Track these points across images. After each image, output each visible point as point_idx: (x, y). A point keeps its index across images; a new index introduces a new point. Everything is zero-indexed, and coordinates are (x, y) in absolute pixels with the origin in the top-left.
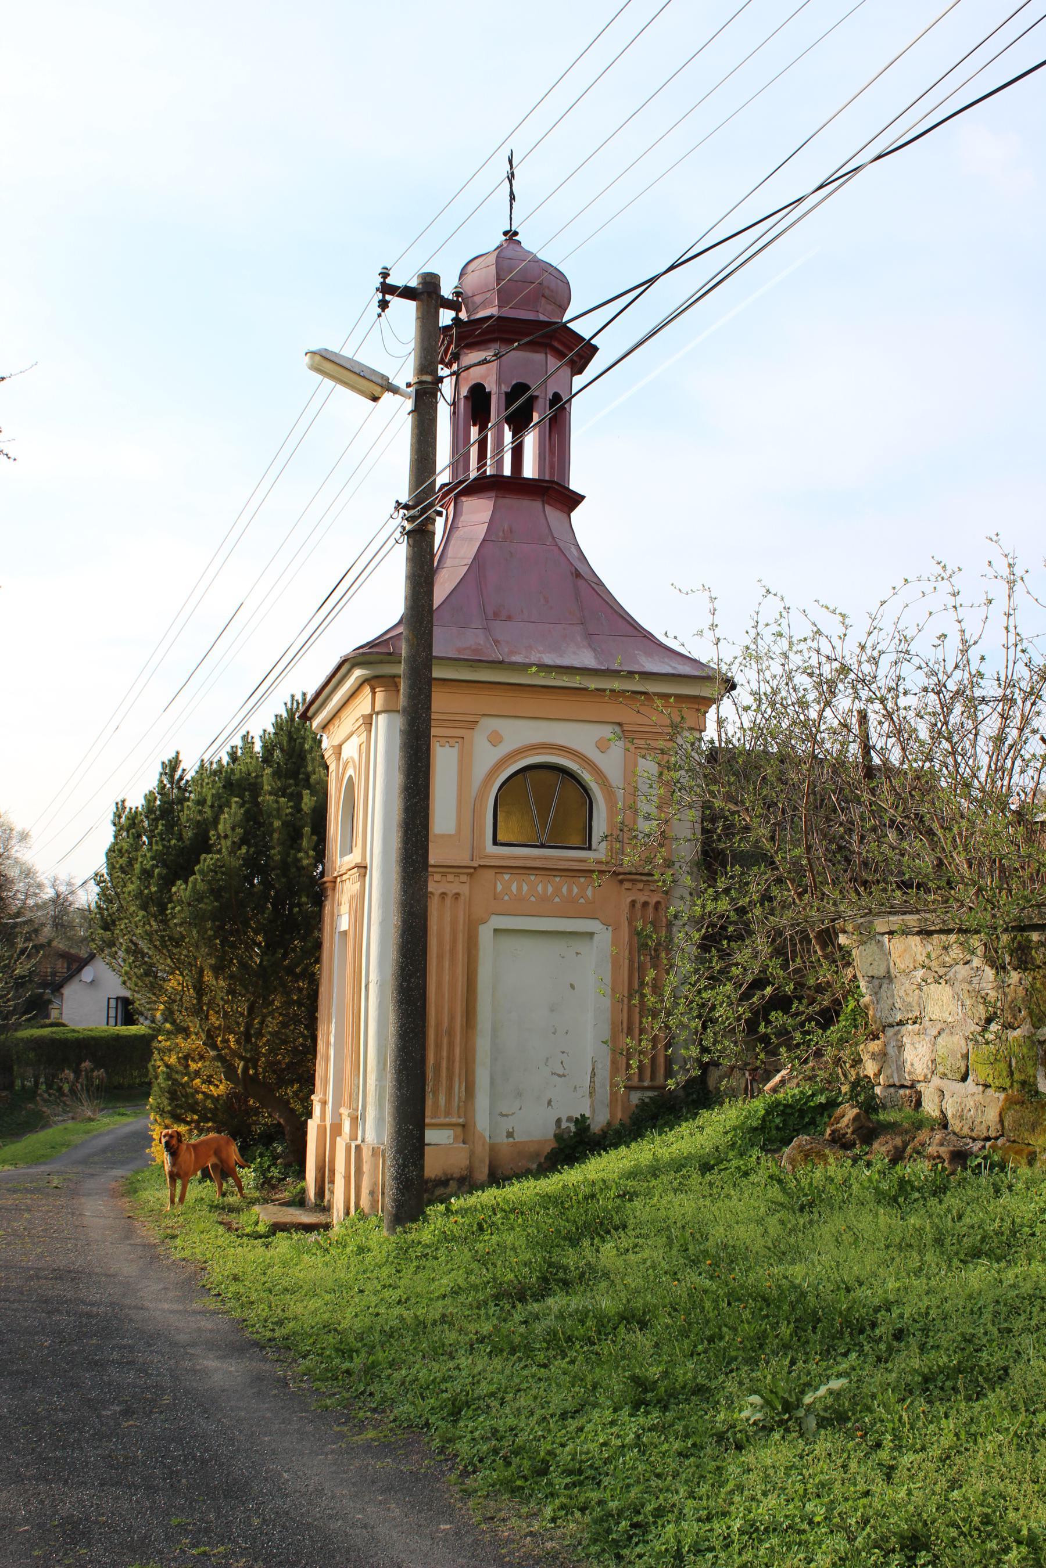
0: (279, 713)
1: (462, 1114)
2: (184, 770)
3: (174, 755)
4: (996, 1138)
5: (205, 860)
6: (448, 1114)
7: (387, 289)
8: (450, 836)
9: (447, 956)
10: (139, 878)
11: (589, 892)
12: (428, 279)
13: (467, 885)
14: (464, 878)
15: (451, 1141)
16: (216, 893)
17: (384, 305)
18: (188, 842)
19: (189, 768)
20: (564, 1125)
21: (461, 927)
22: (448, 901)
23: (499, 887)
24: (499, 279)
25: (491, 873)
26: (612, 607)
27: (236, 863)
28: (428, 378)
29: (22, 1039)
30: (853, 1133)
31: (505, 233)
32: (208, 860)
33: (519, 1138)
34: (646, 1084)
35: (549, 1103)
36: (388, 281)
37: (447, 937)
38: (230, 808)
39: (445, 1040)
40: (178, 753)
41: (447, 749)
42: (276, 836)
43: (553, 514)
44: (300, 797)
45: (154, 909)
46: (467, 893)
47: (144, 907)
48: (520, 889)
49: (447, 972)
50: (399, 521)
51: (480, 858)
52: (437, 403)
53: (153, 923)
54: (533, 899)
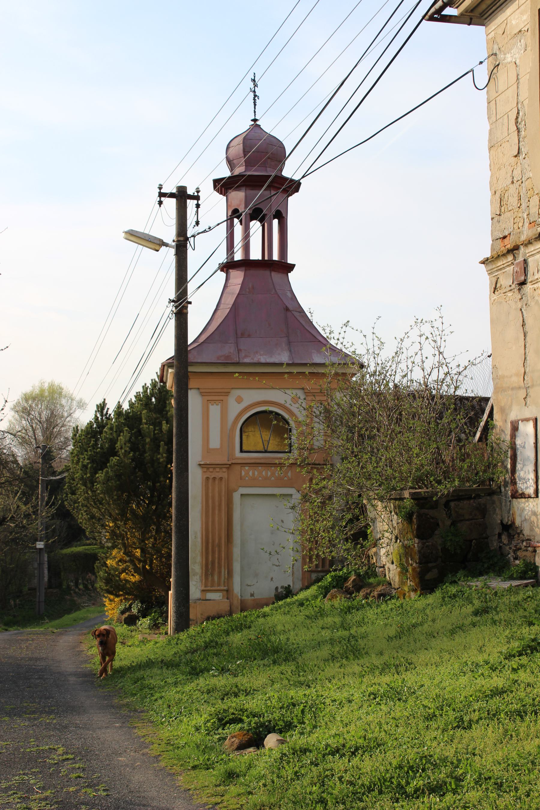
0: (153, 378)
1: (226, 585)
2: (108, 409)
3: (103, 400)
4: (398, 589)
5: (112, 460)
6: (219, 585)
7: (161, 195)
9: (217, 508)
10: (81, 470)
11: (289, 474)
12: (180, 190)
13: (226, 473)
14: (224, 470)
15: (221, 598)
16: (118, 476)
17: (160, 203)
18: (105, 450)
19: (111, 408)
20: (280, 590)
21: (223, 493)
22: (217, 482)
23: (243, 473)
24: (245, 152)
25: (238, 467)
27: (127, 461)
28: (182, 239)
29: (66, 554)
30: (352, 587)
31: (252, 120)
32: (114, 460)
33: (256, 596)
34: (319, 569)
35: (272, 579)
36: (162, 191)
37: (217, 498)
38: (123, 433)
39: (217, 549)
40: (105, 400)
42: (147, 446)
43: (276, 276)
44: (160, 424)
45: (89, 485)
46: (226, 477)
47: (85, 484)
48: (253, 474)
49: (217, 516)
50: (171, 307)
51: (233, 459)
52: (187, 250)
53: (90, 492)
54: (260, 479)
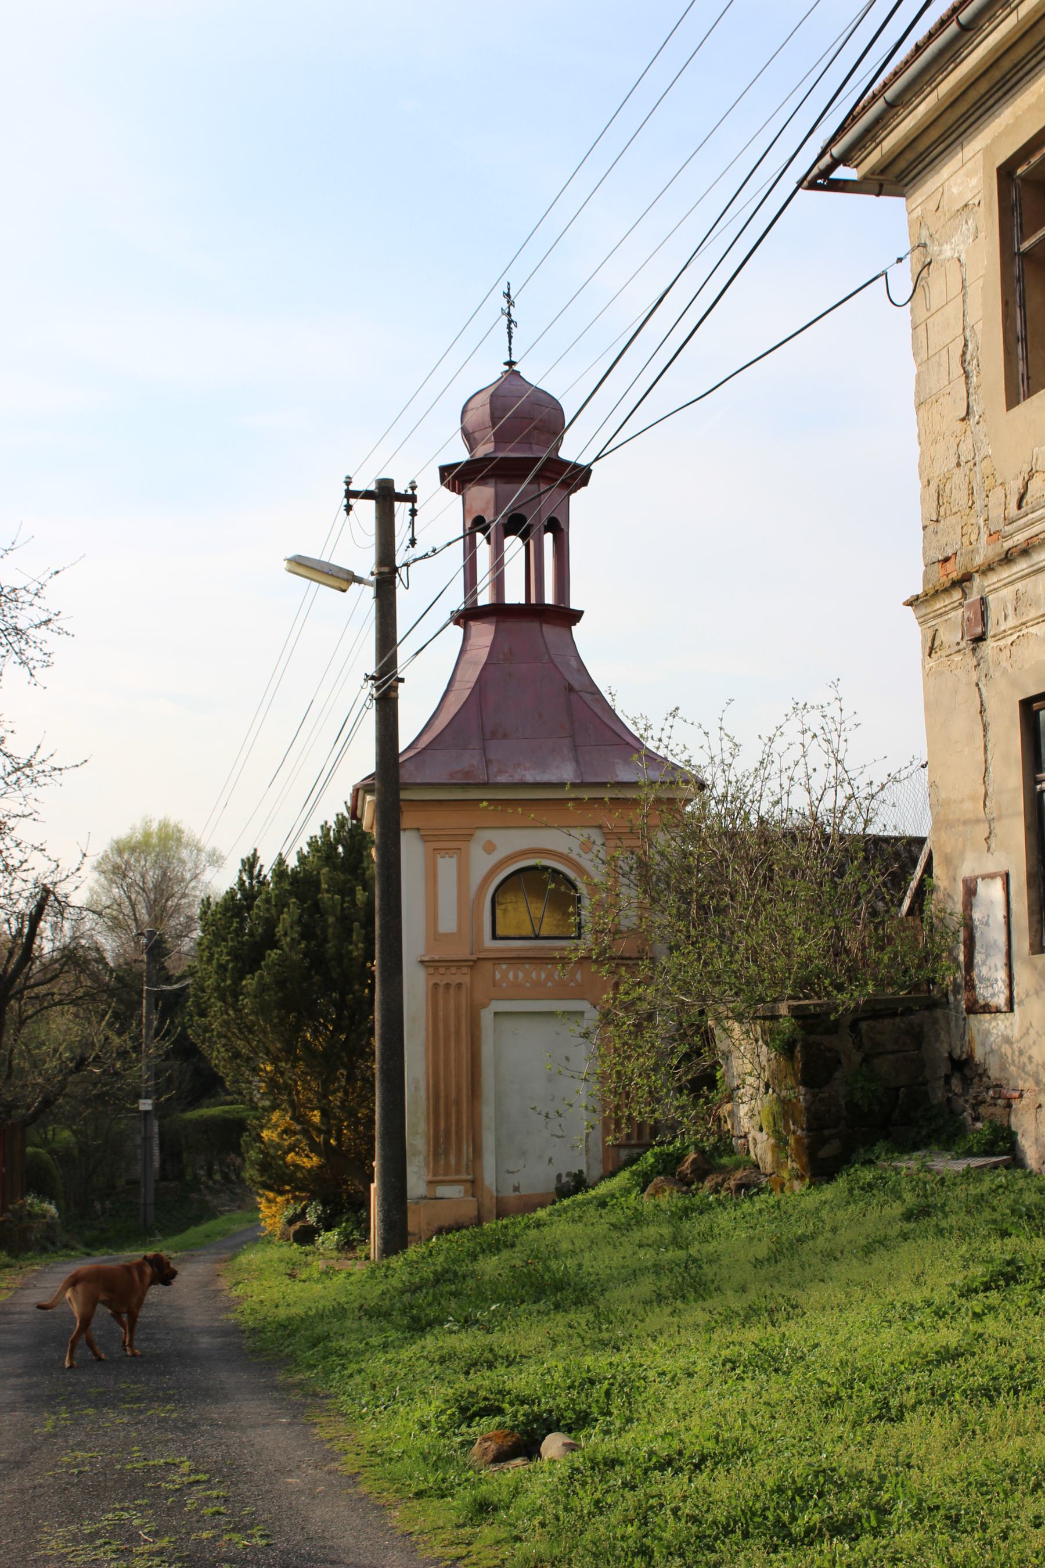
0: (339, 811)
2: (262, 866)
3: (252, 852)
4: (771, 1175)
5: (270, 955)
7: (350, 494)
8: (452, 934)
9: (453, 1037)
10: (216, 973)
11: (578, 976)
12: (383, 485)
14: (465, 970)
15: (462, 1195)
16: (281, 983)
17: (348, 508)
18: (258, 938)
19: (267, 865)
20: (564, 1179)
22: (452, 991)
23: (498, 976)
24: (494, 418)
25: (489, 965)
26: (599, 717)
27: (296, 957)
28: (386, 569)
29: (190, 1121)
30: (691, 1173)
31: (506, 364)
32: (273, 955)
34: (633, 1142)
35: (550, 1160)
36: (352, 488)
39: (453, 1110)
40: (255, 850)
41: (447, 859)
42: (330, 930)
43: (551, 632)
44: (352, 892)
45: (230, 1000)
46: (469, 983)
47: (222, 999)
48: (516, 976)
50: (369, 688)
53: (231, 1012)
54: (528, 985)
